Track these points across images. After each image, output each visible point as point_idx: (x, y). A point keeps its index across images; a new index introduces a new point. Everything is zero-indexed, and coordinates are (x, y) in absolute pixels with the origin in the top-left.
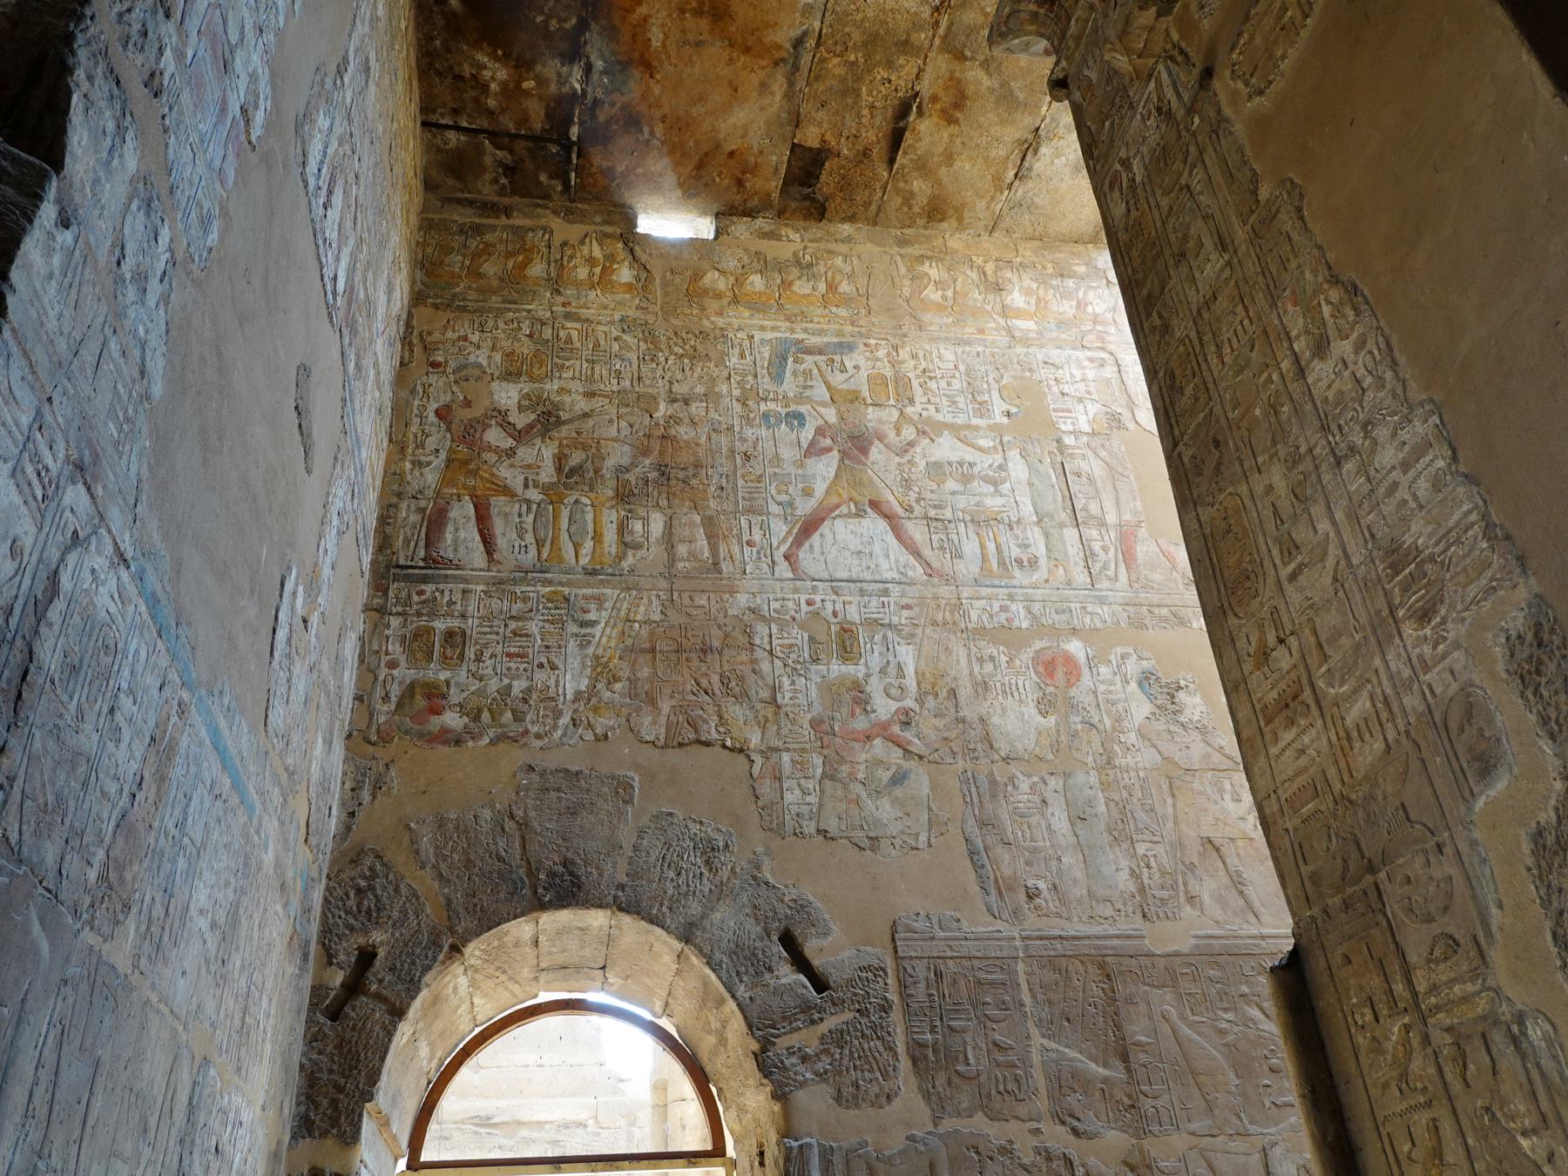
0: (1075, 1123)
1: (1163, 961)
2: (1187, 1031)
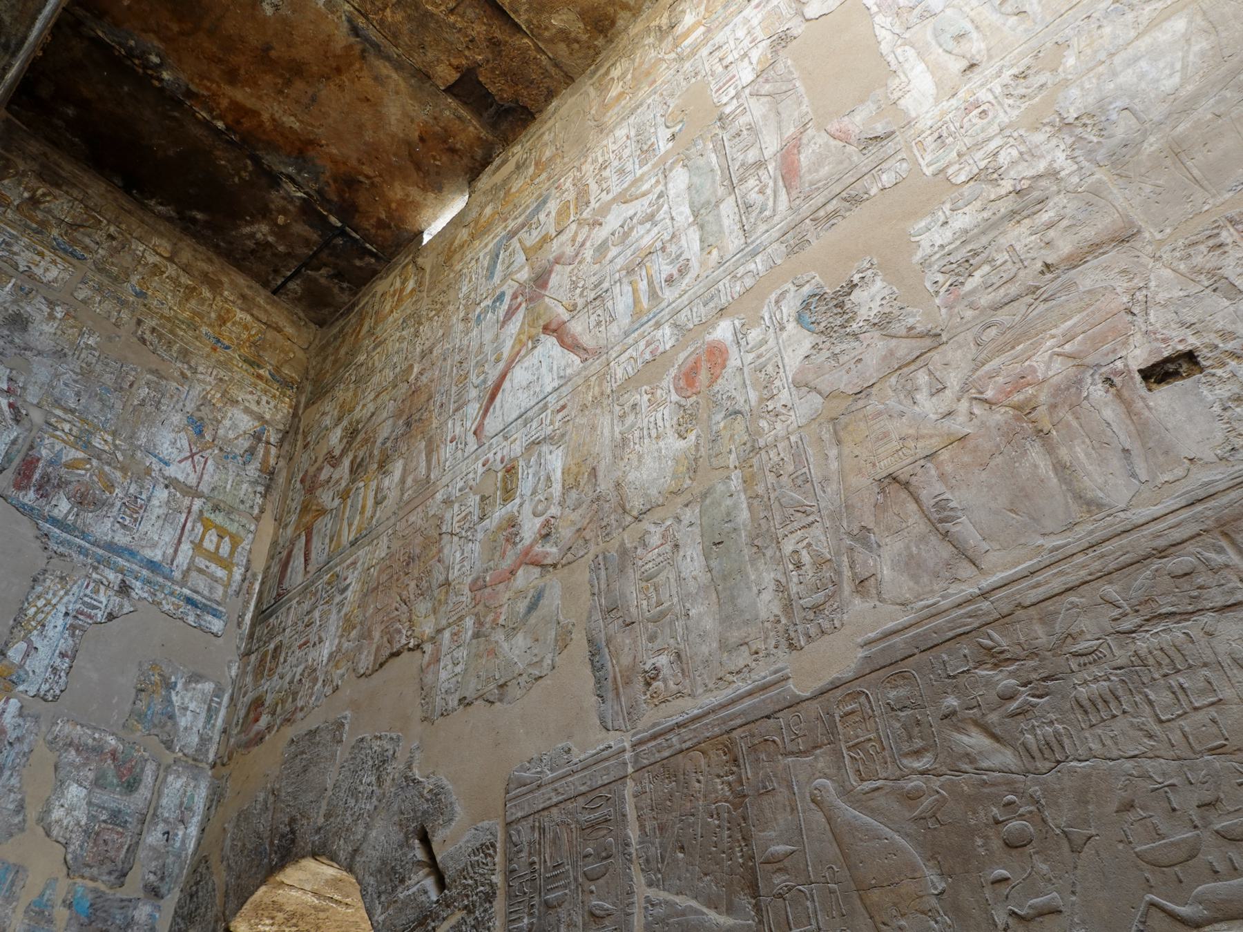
1: (815, 705)
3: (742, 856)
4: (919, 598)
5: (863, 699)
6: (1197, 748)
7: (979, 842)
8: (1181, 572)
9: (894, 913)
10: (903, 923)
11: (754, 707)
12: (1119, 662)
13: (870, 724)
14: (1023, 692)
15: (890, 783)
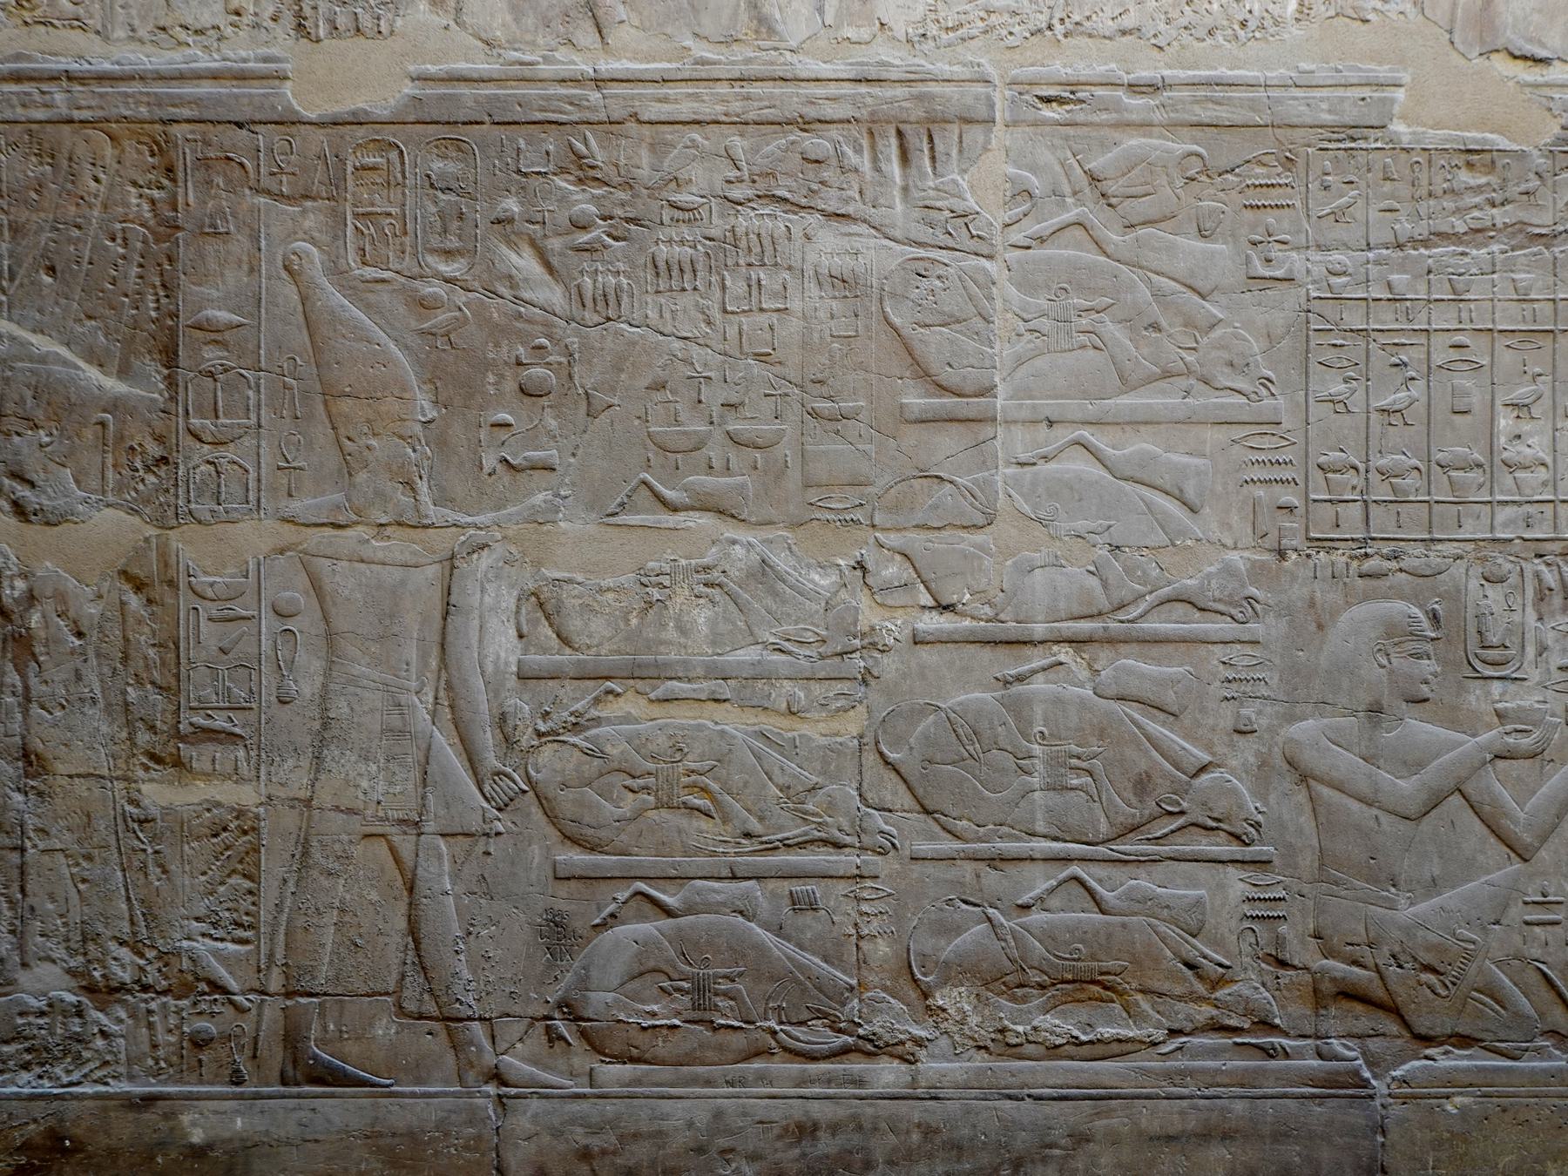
0: (23, 492)
1: (320, 135)
2: (338, 299)
3: (157, 309)
4: (512, 44)
5: (394, 155)
6: (746, 349)
7: (491, 378)
8: (813, 157)
9: (366, 430)
10: (374, 442)
11: (218, 101)
12: (713, 233)
13: (395, 194)
14: (599, 227)
15: (403, 280)
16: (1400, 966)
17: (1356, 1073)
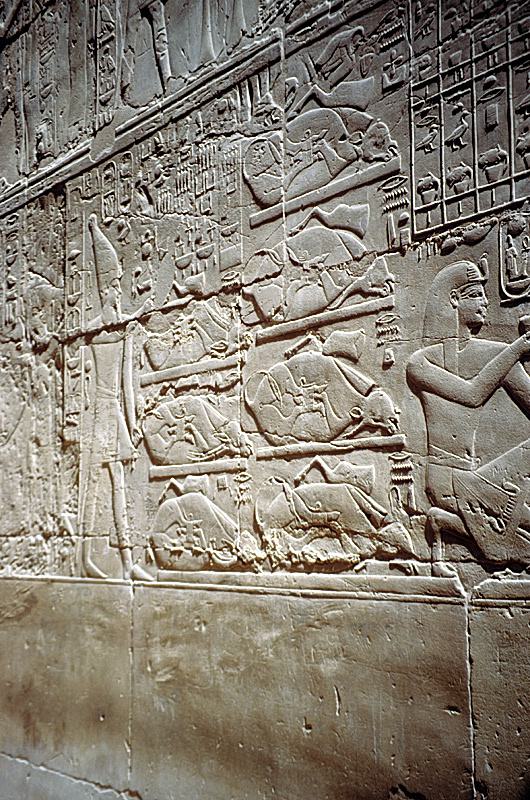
16: (474, 511)
17: (452, 586)
